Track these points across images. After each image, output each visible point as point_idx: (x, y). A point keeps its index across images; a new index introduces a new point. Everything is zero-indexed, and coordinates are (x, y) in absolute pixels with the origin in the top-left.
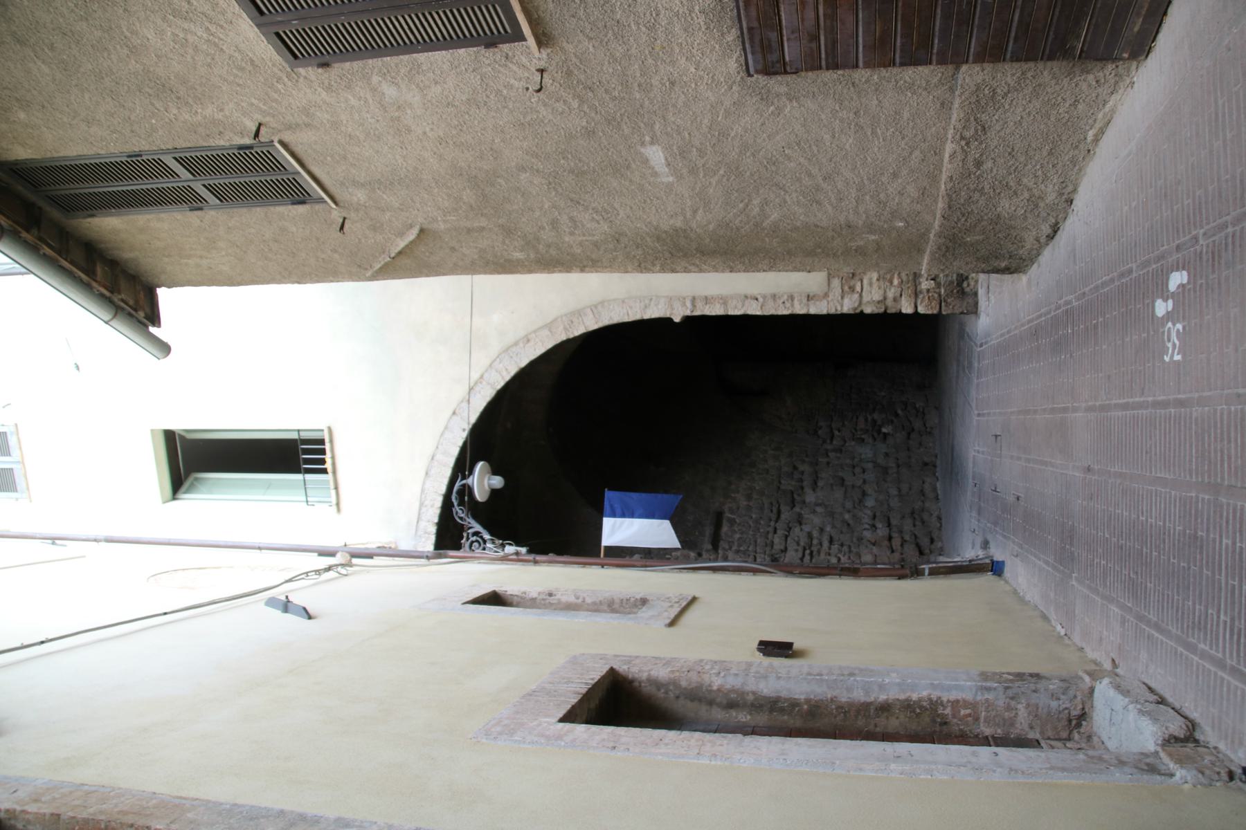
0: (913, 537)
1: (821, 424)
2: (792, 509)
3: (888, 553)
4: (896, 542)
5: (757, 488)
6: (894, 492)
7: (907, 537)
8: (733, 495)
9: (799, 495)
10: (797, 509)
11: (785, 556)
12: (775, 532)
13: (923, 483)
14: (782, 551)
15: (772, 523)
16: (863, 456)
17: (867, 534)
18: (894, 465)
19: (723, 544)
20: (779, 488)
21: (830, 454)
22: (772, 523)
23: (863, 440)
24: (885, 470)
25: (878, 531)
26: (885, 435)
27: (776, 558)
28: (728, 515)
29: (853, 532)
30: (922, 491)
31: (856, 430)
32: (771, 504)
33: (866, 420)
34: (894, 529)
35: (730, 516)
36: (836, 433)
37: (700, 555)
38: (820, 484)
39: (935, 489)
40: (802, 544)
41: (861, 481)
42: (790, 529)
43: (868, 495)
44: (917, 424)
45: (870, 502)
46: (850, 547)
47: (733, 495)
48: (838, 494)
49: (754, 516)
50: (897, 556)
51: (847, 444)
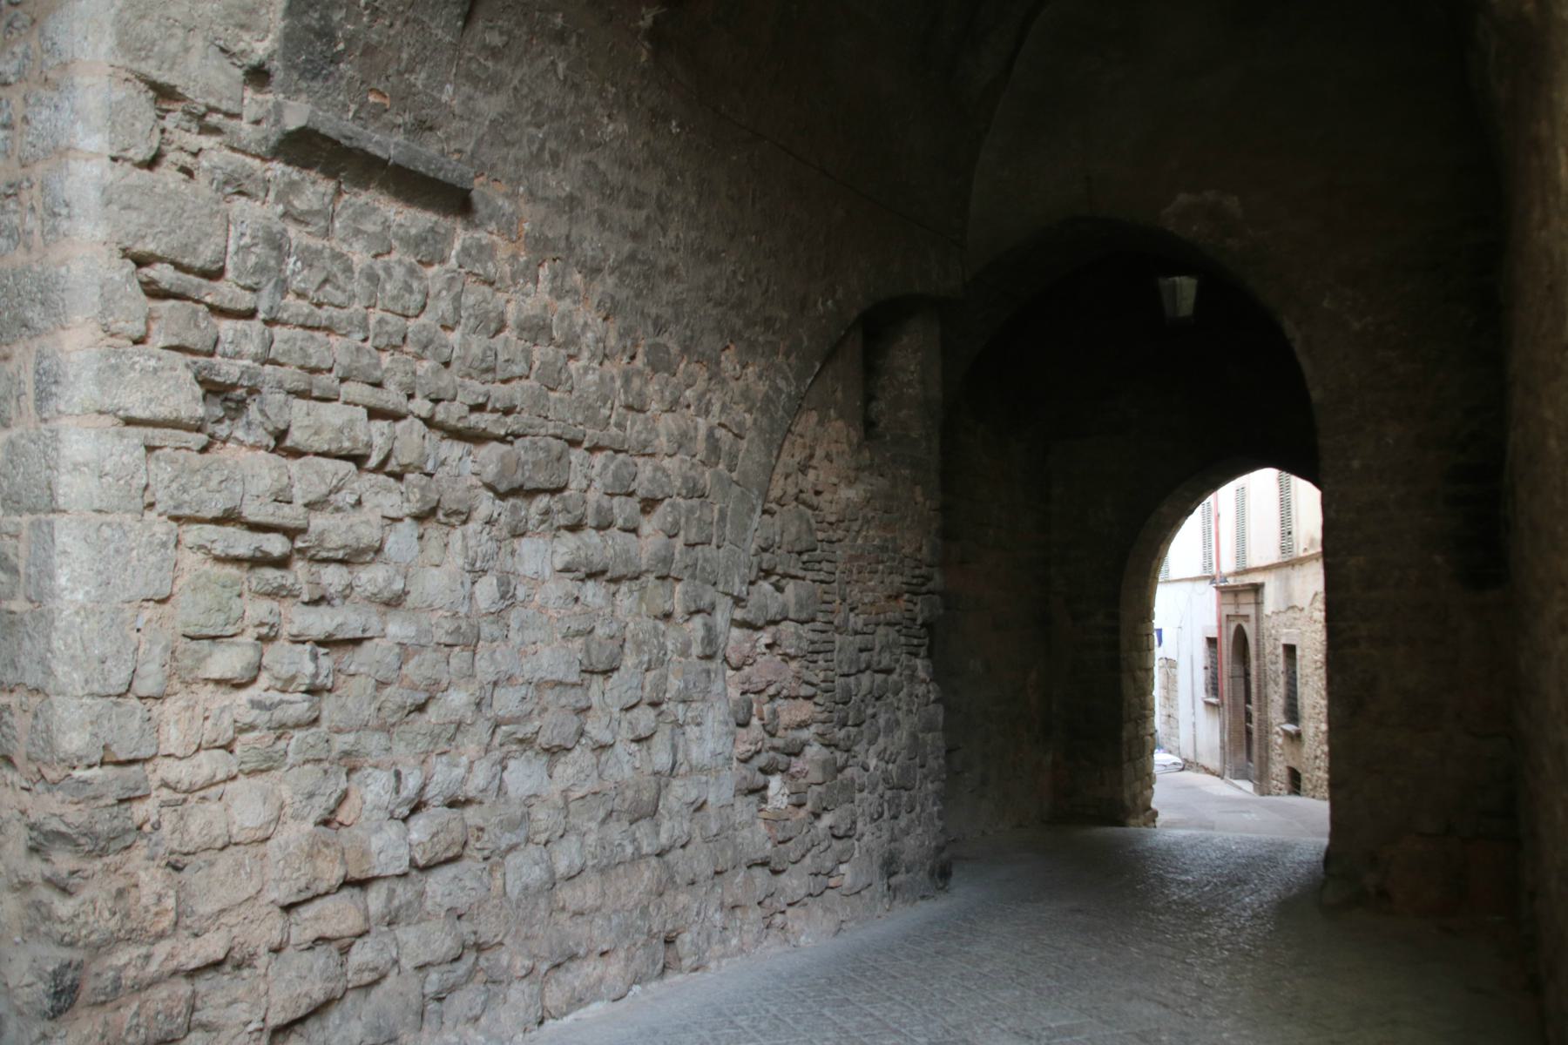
0: (367, 977)
1: (790, 587)
2: (490, 487)
3: (284, 894)
4: (339, 915)
5: (573, 366)
6: (565, 858)
7: (362, 954)
8: (544, 272)
9: (547, 512)
10: (486, 505)
11: (254, 447)
12: (374, 413)
13: (603, 954)
14: (281, 435)
15: (421, 406)
16: (692, 731)
17: (374, 789)
18: (664, 839)
19: (315, 190)
20: (574, 443)
21: (698, 621)
22: (421, 406)
23: (744, 724)
24: (648, 812)
25: (393, 830)
26: (759, 791)
27: (241, 405)
28: (461, 236)
29: (386, 728)
30: (573, 957)
31: (772, 698)
32: (507, 411)
33: (803, 725)
34: (404, 892)
35: (457, 245)
36: (765, 638)
37: (258, 76)
38: (593, 593)
39: (578, 1002)
40: (318, 521)
41: (606, 737)
42: (399, 477)
43: (550, 767)
44: (794, 883)
45: (523, 776)
46: (315, 721)
47: (544, 272)
48: (553, 660)
49: (454, 337)
50: (270, 929)
51: (730, 673)
